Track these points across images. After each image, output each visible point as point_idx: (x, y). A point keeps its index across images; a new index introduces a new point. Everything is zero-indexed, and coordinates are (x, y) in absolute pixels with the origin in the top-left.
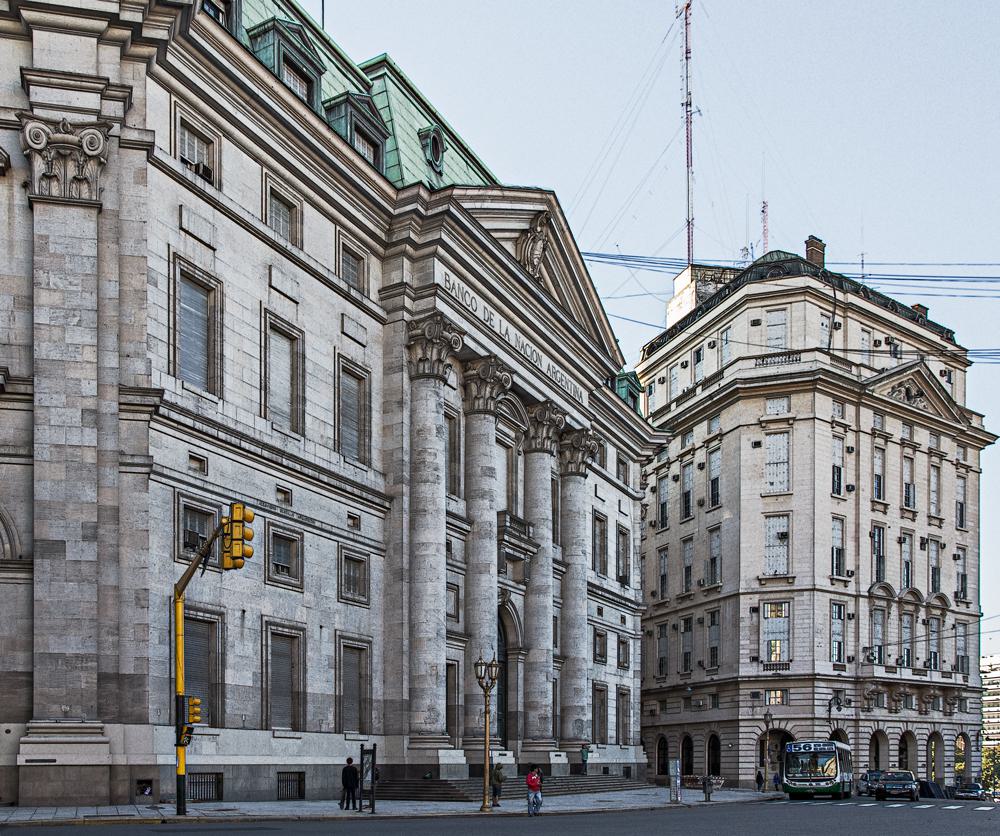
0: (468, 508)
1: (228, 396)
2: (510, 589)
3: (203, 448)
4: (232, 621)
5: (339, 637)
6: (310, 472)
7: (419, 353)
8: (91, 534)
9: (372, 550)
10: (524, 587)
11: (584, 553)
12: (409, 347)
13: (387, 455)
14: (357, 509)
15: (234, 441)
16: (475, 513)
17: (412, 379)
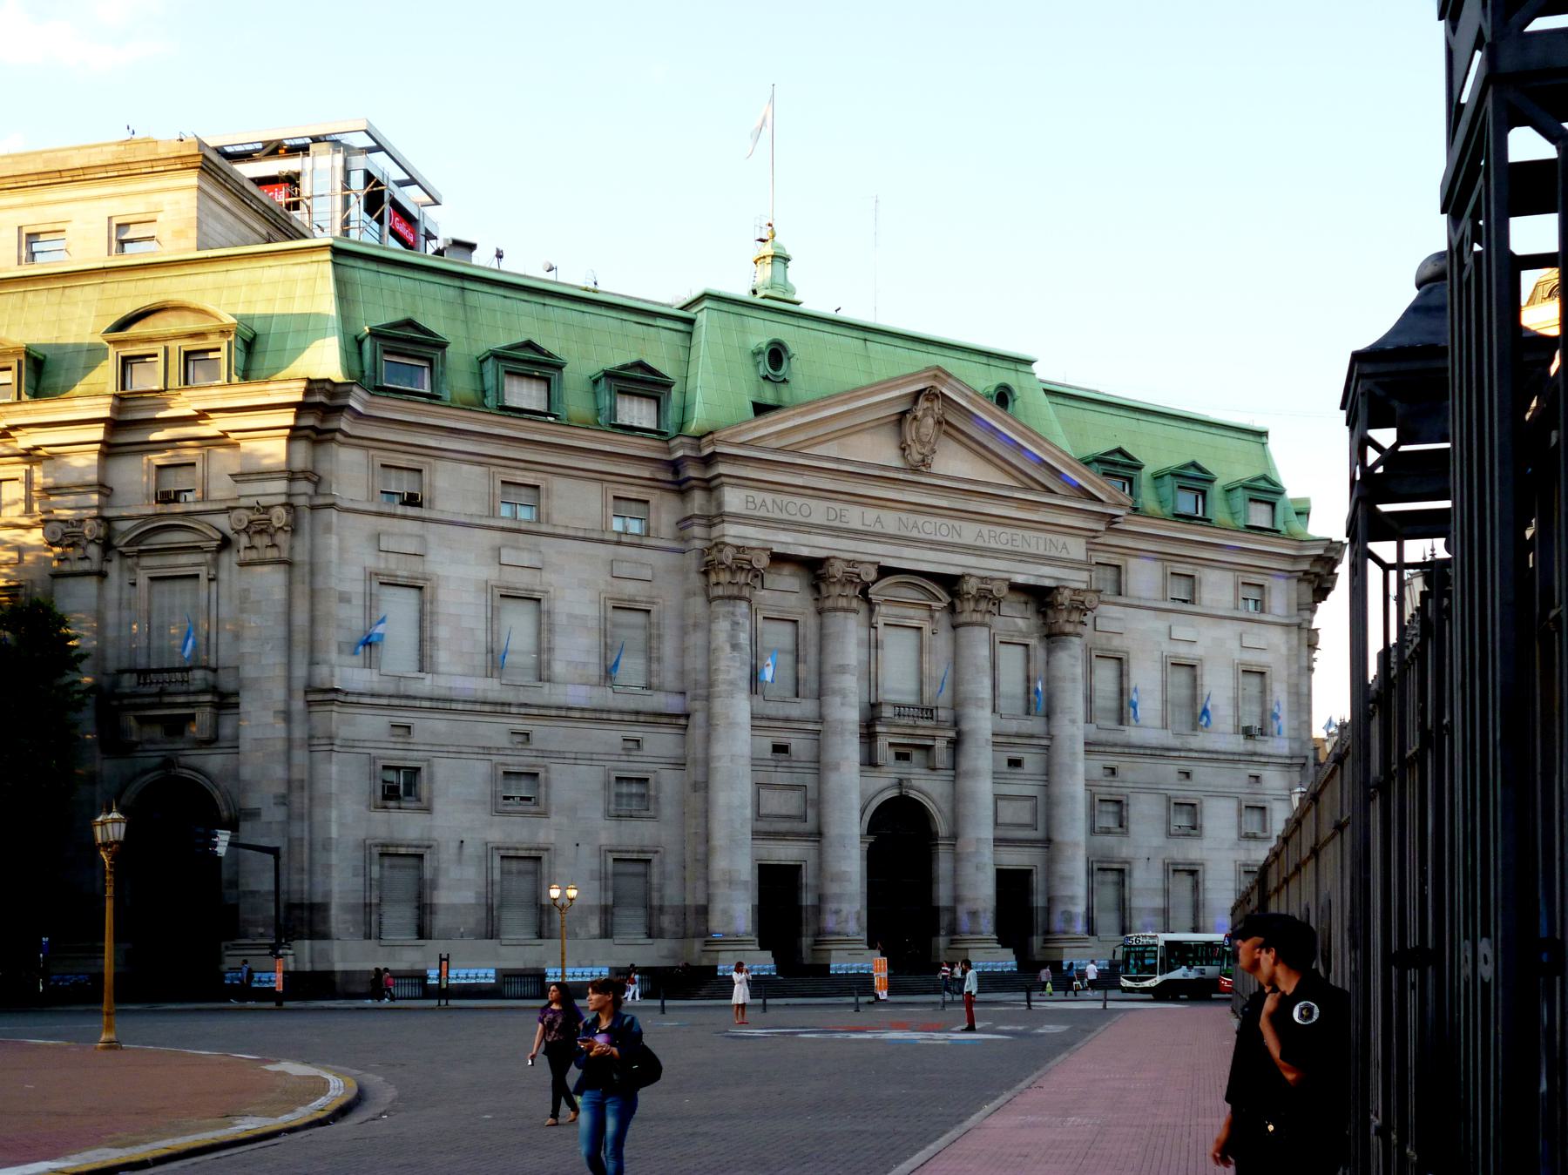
0: (820, 706)
1: (442, 669)
2: (911, 776)
3: (403, 718)
4: (447, 853)
5: (604, 852)
6: (553, 712)
7: (713, 578)
8: (283, 800)
9: (661, 766)
10: (952, 773)
11: (1073, 721)
12: (706, 573)
13: (682, 674)
14: (636, 732)
15: (442, 704)
16: (828, 711)
17: (710, 600)
